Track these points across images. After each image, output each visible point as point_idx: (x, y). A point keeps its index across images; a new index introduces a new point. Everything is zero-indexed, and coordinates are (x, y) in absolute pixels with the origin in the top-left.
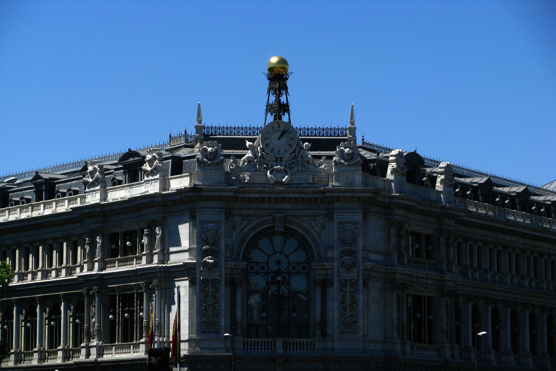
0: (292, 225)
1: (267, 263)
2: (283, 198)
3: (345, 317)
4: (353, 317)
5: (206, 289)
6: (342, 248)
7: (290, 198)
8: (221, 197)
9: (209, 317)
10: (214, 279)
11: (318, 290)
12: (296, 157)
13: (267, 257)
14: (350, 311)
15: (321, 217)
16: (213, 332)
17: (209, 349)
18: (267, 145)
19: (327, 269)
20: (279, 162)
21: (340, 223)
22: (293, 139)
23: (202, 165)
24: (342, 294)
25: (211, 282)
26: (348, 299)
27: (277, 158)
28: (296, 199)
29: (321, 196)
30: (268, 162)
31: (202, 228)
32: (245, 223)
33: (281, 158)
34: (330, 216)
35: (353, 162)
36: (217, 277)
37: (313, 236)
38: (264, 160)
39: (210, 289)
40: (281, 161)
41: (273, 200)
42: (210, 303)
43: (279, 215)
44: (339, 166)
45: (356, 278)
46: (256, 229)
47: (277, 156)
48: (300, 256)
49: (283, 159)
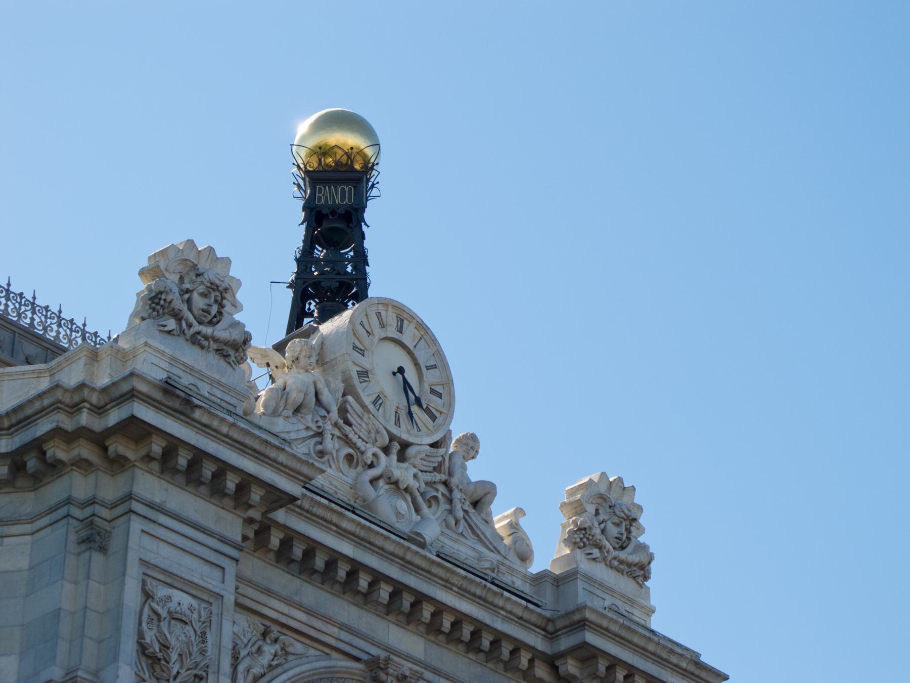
2: (420, 598)
7: (440, 609)
8: (247, 481)
12: (437, 469)
18: (364, 374)
20: (394, 457)
22: (440, 396)
23: (171, 324)
27: (392, 438)
28: (460, 619)
29: (536, 641)
30: (359, 443)
31: (148, 596)
32: (269, 650)
33: (405, 446)
35: (635, 558)
38: (347, 428)
40: (402, 457)
41: (384, 592)
43: (407, 667)
44: (596, 552)
47: (394, 430)
49: (411, 451)
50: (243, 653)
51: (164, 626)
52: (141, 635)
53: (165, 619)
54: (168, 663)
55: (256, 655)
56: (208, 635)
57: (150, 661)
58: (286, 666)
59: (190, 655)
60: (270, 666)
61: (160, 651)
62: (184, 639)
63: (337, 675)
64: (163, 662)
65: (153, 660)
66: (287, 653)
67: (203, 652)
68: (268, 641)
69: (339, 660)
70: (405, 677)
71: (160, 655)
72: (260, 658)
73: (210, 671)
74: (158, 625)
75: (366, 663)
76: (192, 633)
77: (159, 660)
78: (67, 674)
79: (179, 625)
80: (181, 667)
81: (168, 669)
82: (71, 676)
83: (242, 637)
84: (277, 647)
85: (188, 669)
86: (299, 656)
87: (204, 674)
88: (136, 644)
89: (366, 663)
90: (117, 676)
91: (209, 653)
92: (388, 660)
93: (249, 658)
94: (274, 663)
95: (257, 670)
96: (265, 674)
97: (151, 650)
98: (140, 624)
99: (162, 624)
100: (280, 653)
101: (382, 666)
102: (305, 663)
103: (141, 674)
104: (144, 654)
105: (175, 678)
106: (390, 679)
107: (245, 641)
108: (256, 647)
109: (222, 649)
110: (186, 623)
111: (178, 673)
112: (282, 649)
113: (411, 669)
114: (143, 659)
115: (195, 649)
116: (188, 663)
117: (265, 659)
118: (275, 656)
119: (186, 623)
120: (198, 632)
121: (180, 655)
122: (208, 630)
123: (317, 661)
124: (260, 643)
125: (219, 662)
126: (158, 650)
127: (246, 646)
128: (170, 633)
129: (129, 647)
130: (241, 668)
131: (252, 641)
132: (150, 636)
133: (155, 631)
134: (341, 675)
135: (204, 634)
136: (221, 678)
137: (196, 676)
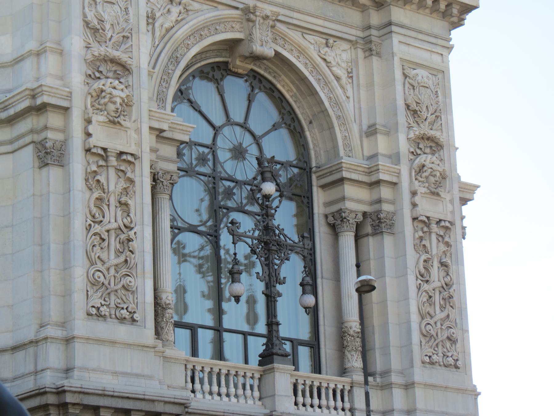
0: (283, 47)
1: (212, 148)
3: (432, 322)
4: (447, 324)
5: (102, 179)
6: (417, 131)
9: (108, 269)
10: (122, 153)
11: (347, 240)
13: (211, 132)
14: (443, 308)
15: (345, 46)
16: (122, 320)
17: (115, 374)
19: (378, 183)
21: (409, 65)
24: (424, 257)
25: (113, 161)
26: (435, 271)
34: (370, 45)
36: (132, 149)
37: (331, 90)
39: (113, 183)
42: (114, 225)
45: (449, 218)
46: (202, 38)
48: (279, 147)
50: (158, 15)
51: (100, 8)
52: (85, 16)
53: (99, 3)
54: (104, 31)
55: (166, 15)
56: (130, 9)
57: (93, 31)
58: (188, 19)
59: (118, 24)
60: (177, 20)
61: (99, 24)
62: (114, 14)
63: (223, 20)
64: (101, 31)
65: (95, 31)
66: (187, 11)
67: (127, 21)
68: (174, 4)
69: (224, 10)
70: (267, 17)
71: (98, 27)
72: (169, 17)
73: (133, 32)
74: (96, 7)
75: (242, 10)
76: (119, 11)
77: (98, 30)
78: (41, 45)
79: (108, 5)
80: (114, 33)
81: (104, 34)
82: (43, 46)
83: (157, 4)
84: (181, 8)
85: (118, 33)
86: (197, 11)
87: (129, 35)
88: (82, 23)
89: (242, 10)
90: (72, 44)
91: (131, 21)
92: (255, 7)
93: (162, 17)
94: (179, 19)
95: (167, 25)
96: (174, 26)
97: (92, 24)
98: (84, 8)
99: (98, 6)
100: (183, 11)
101: (252, 11)
102: (201, 16)
103: (88, 40)
104: (88, 27)
105: (110, 40)
106: (258, 19)
107: (159, 6)
108: (167, 9)
109: (140, 17)
110: (114, 4)
111: (112, 36)
112: (184, 8)
113: (271, 11)
114: (88, 31)
115: (122, 20)
116: (118, 29)
117: (174, 16)
118: (180, 13)
119: (114, 4)
120: (123, 9)
121: (112, 25)
122: (129, 6)
123: (209, 13)
124: (169, 6)
125: (138, 25)
126: (97, 24)
127: (160, 9)
128: (104, 12)
129: (77, 24)
130: (157, 25)
131: (164, 5)
132: (91, 16)
133: (94, 10)
134: (226, 20)
135: (126, 9)
136: (141, 35)
137: (124, 37)
